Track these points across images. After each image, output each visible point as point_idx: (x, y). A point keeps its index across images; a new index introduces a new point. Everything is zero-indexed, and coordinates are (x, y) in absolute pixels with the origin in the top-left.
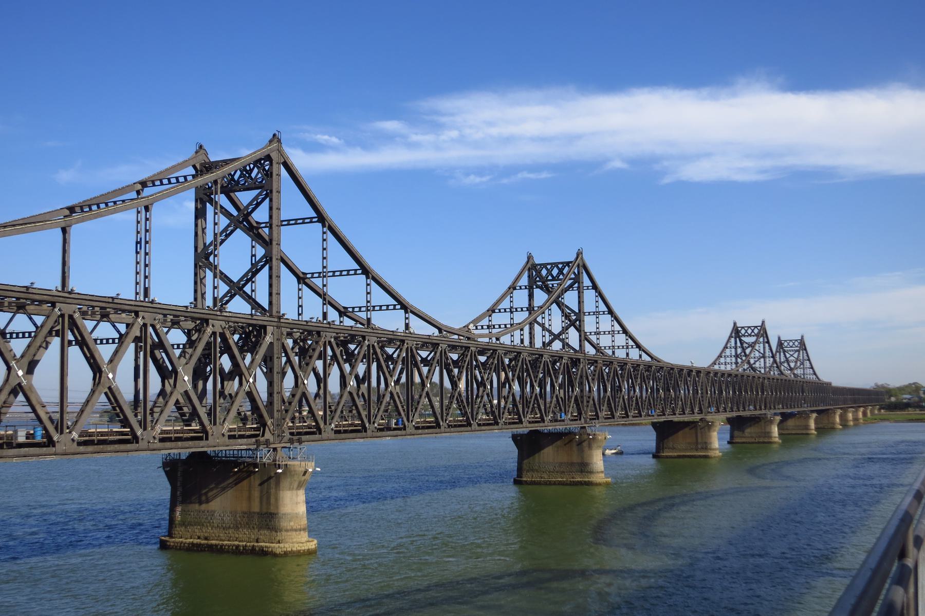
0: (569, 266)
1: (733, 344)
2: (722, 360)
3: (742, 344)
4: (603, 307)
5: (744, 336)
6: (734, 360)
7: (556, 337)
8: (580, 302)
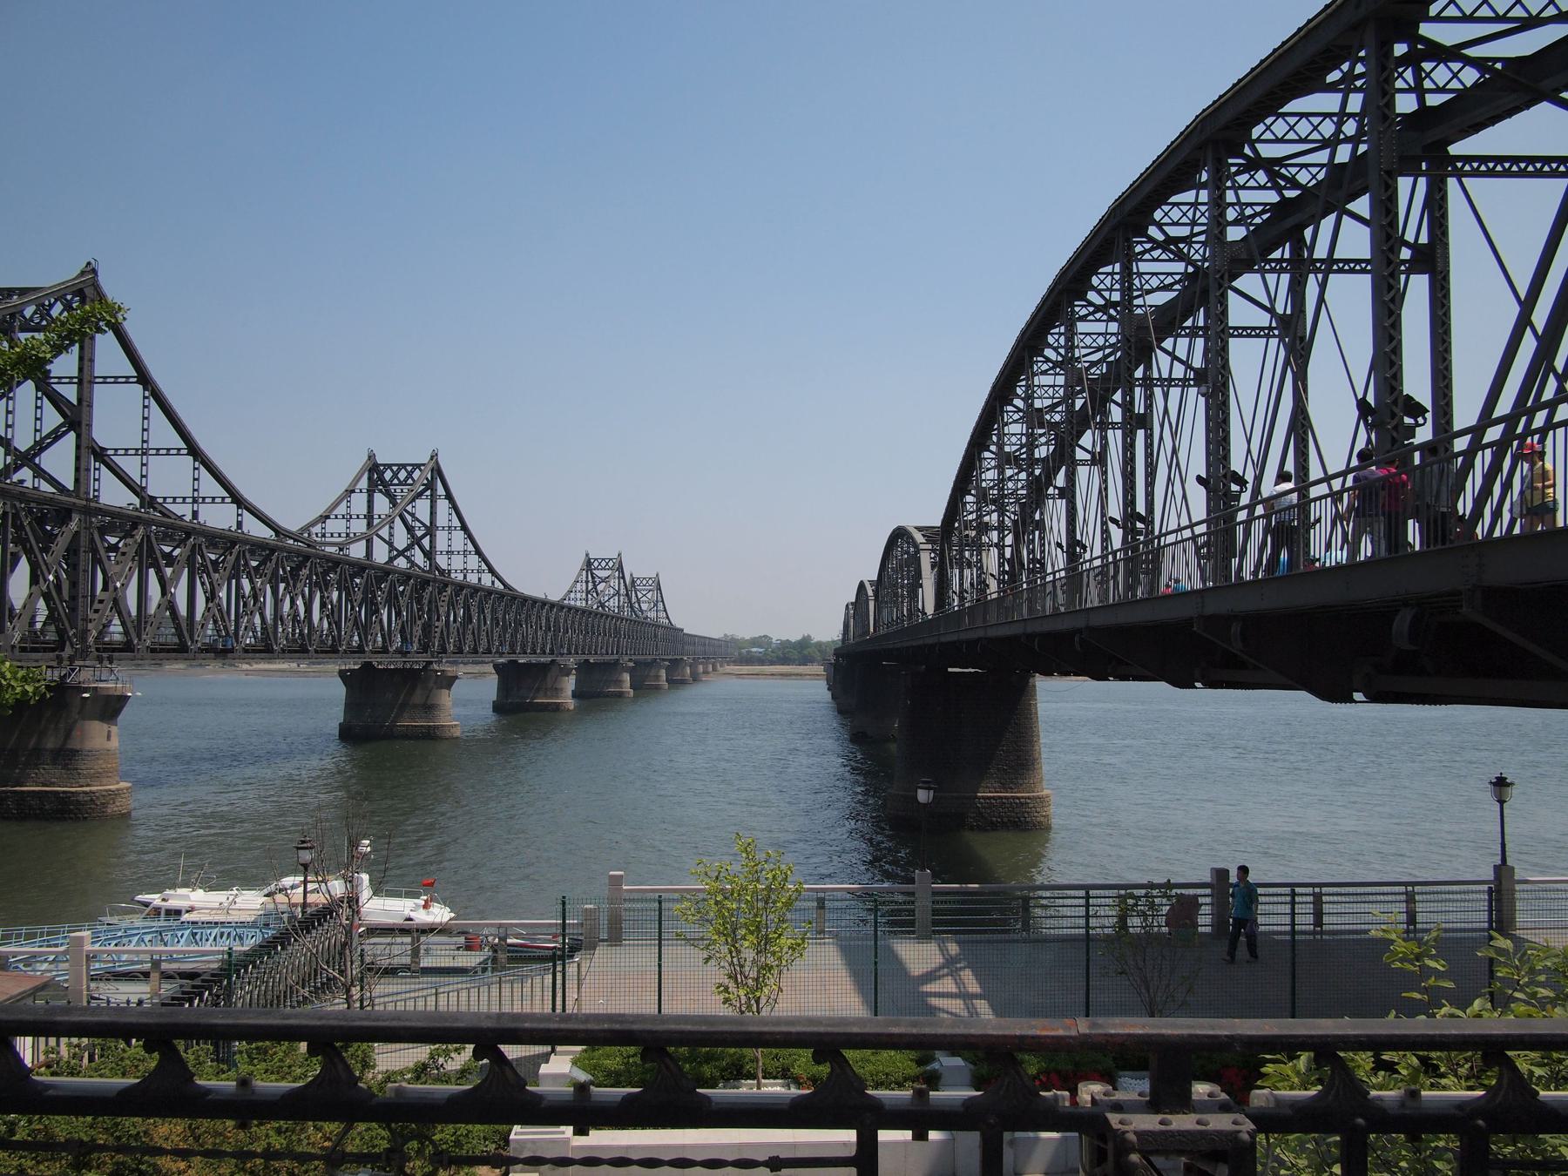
0: (420, 470)
1: (584, 579)
2: (572, 595)
3: (593, 578)
4: (456, 523)
5: (597, 569)
6: (584, 594)
7: (401, 553)
8: (433, 513)
